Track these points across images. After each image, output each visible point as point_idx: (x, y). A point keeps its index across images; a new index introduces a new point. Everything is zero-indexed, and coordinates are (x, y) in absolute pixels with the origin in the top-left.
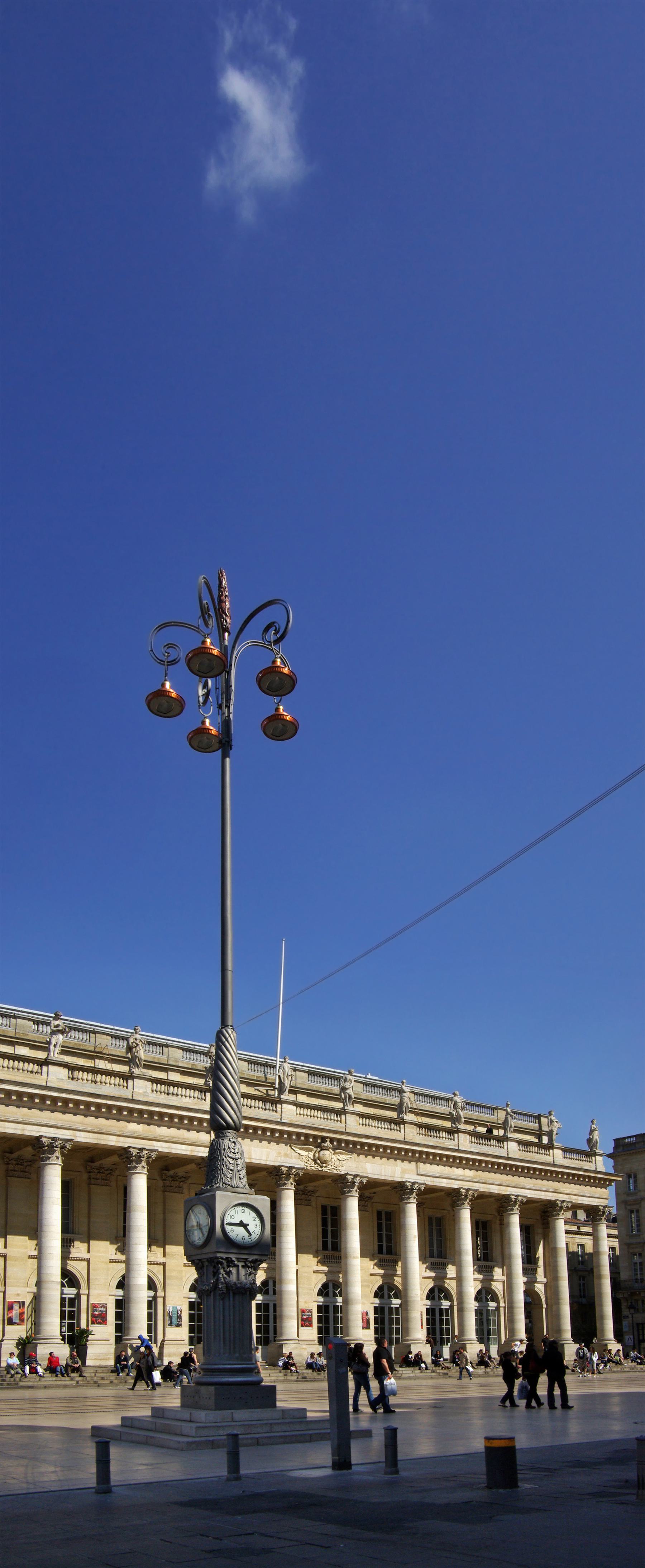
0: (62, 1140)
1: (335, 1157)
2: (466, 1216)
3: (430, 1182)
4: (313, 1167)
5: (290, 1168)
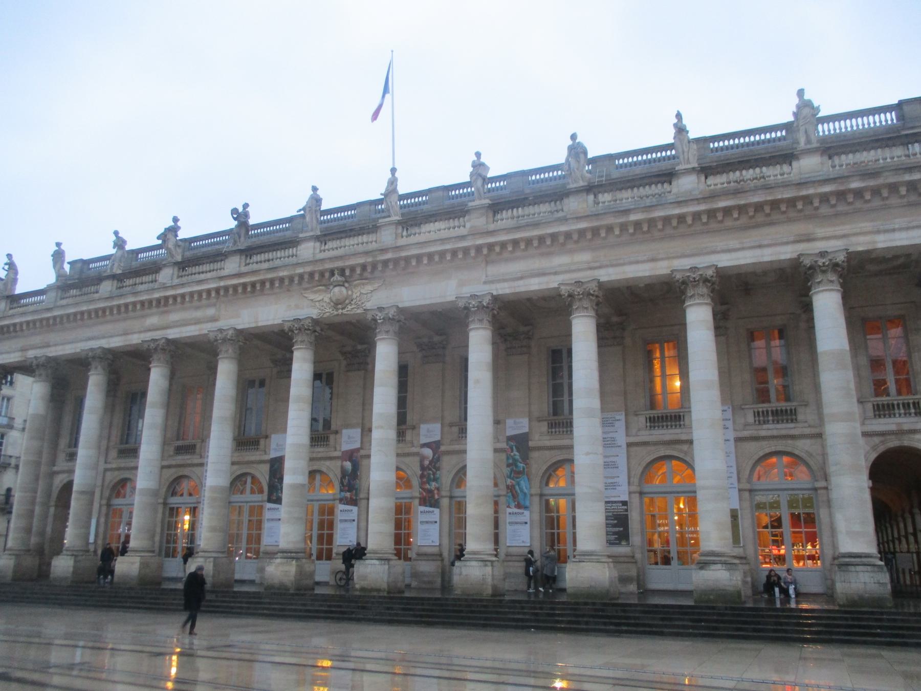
3: (504, 289)
4: (329, 312)
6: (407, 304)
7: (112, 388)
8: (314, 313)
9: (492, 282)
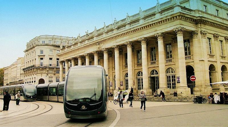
4: (98, 50)
7: (120, 53)
9: (117, 42)
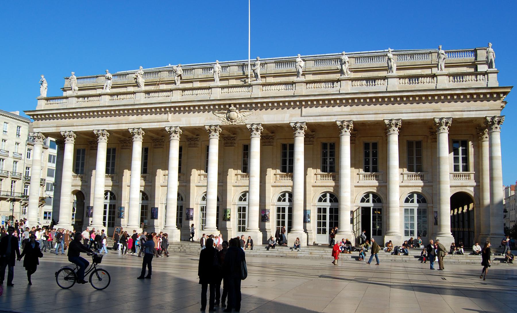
0: (498, 117)
1: (240, 115)
2: (394, 139)
3: (312, 120)
5: (210, 126)
6: (266, 123)
8: (220, 123)
